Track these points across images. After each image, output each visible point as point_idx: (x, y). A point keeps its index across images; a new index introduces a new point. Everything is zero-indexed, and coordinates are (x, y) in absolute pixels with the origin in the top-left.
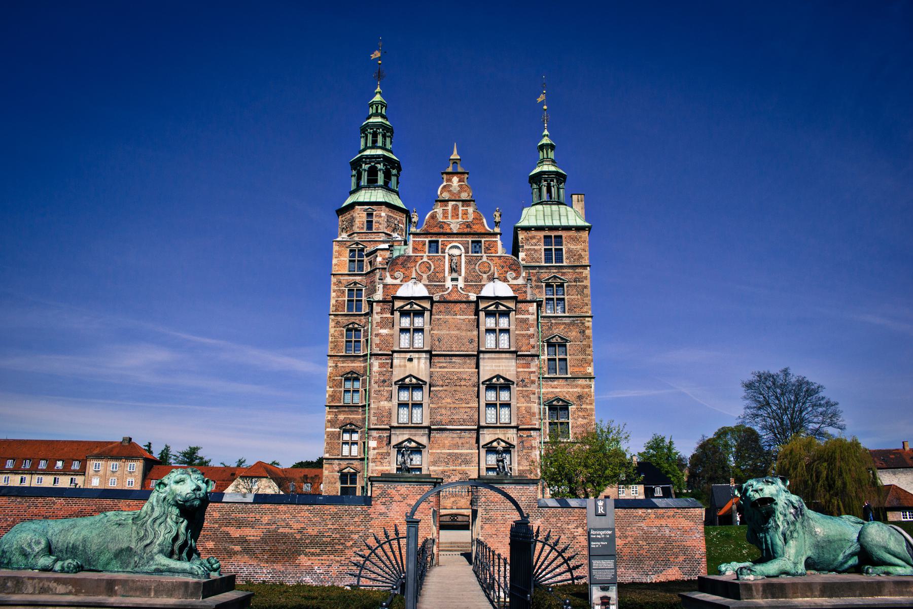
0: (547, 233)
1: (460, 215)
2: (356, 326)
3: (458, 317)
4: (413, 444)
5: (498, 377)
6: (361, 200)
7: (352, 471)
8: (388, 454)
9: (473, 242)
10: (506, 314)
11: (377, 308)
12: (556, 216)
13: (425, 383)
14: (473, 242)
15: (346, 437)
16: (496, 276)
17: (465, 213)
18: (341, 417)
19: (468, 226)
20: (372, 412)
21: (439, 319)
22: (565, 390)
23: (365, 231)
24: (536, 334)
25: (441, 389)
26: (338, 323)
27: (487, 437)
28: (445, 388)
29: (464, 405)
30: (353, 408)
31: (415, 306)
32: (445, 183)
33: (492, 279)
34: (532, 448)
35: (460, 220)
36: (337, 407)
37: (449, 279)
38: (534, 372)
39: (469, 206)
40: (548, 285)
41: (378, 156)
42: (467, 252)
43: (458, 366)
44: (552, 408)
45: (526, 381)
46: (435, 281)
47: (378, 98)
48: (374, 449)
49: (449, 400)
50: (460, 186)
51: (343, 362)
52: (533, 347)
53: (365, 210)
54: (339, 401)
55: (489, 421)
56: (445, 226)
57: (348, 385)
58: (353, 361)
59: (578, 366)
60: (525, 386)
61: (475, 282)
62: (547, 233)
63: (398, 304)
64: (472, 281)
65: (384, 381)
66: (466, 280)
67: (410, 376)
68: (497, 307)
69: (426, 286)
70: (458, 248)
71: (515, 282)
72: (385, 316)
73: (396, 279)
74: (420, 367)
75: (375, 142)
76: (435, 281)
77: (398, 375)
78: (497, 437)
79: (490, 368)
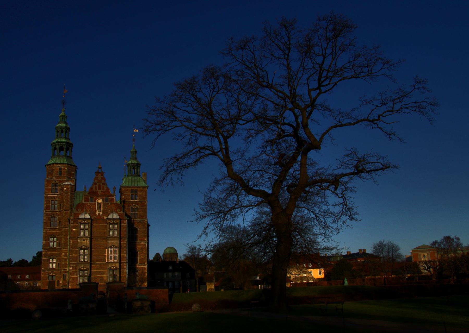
6: (57, 162)
11: (72, 221)
17: (103, 188)
30: (54, 249)
33: (112, 212)
36: (47, 249)
40: (132, 208)
41: (64, 142)
42: (103, 202)
46: (92, 213)
57: (52, 239)
61: (106, 213)
62: (132, 189)
63: (80, 221)
66: (103, 212)
69: (89, 214)
71: (120, 213)
76: (92, 213)
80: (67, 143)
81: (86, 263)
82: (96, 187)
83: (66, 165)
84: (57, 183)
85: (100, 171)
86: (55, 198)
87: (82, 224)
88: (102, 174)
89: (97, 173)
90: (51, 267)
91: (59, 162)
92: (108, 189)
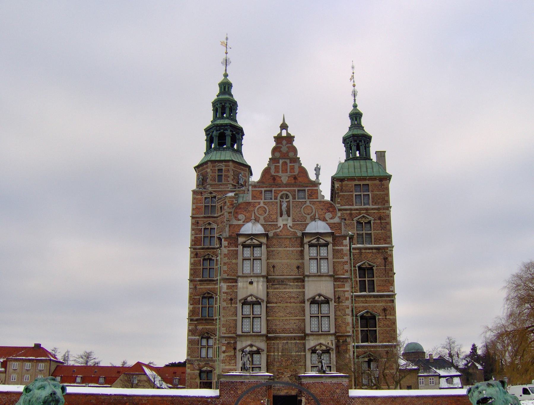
0: (357, 182)
1: (289, 170)
2: (210, 257)
3: (288, 249)
4: (255, 349)
5: (320, 295)
7: (209, 369)
8: (235, 356)
9: (298, 190)
10: (326, 245)
11: (225, 243)
12: (364, 169)
13: (263, 301)
14: (298, 190)
15: (204, 342)
16: (317, 216)
17: (292, 168)
18: (200, 327)
19: (295, 178)
20: (222, 323)
21: (272, 251)
22: (374, 304)
23: (217, 183)
24: (349, 261)
25: (275, 305)
26: (197, 254)
27: (311, 343)
28: (279, 305)
29: (293, 318)
31: (254, 241)
33: (313, 219)
35: (288, 173)
36: (197, 320)
37: (280, 219)
38: (348, 291)
40: (358, 222)
41: (226, 125)
43: (288, 286)
45: (342, 298)
48: (224, 352)
49: (281, 314)
50: (288, 147)
51: (201, 285)
52: (347, 272)
54: (198, 315)
55: (313, 329)
56: (277, 178)
58: (208, 284)
59: (383, 286)
60: (341, 302)
62: (357, 182)
63: (241, 240)
64: (298, 221)
65: (231, 300)
67: (251, 295)
68: (318, 241)
69: (262, 225)
71: (332, 221)
72: (231, 249)
73: (239, 220)
74: (259, 289)
77: (241, 295)
78: (319, 342)
79: (312, 289)
80: (231, 126)
81: (258, 335)
82: (277, 168)
83: (231, 163)
84: (215, 197)
85: (284, 133)
86: (209, 224)
87: (249, 246)
88: (290, 138)
89: (278, 139)
90: (204, 354)
91: (218, 159)
92: (304, 172)
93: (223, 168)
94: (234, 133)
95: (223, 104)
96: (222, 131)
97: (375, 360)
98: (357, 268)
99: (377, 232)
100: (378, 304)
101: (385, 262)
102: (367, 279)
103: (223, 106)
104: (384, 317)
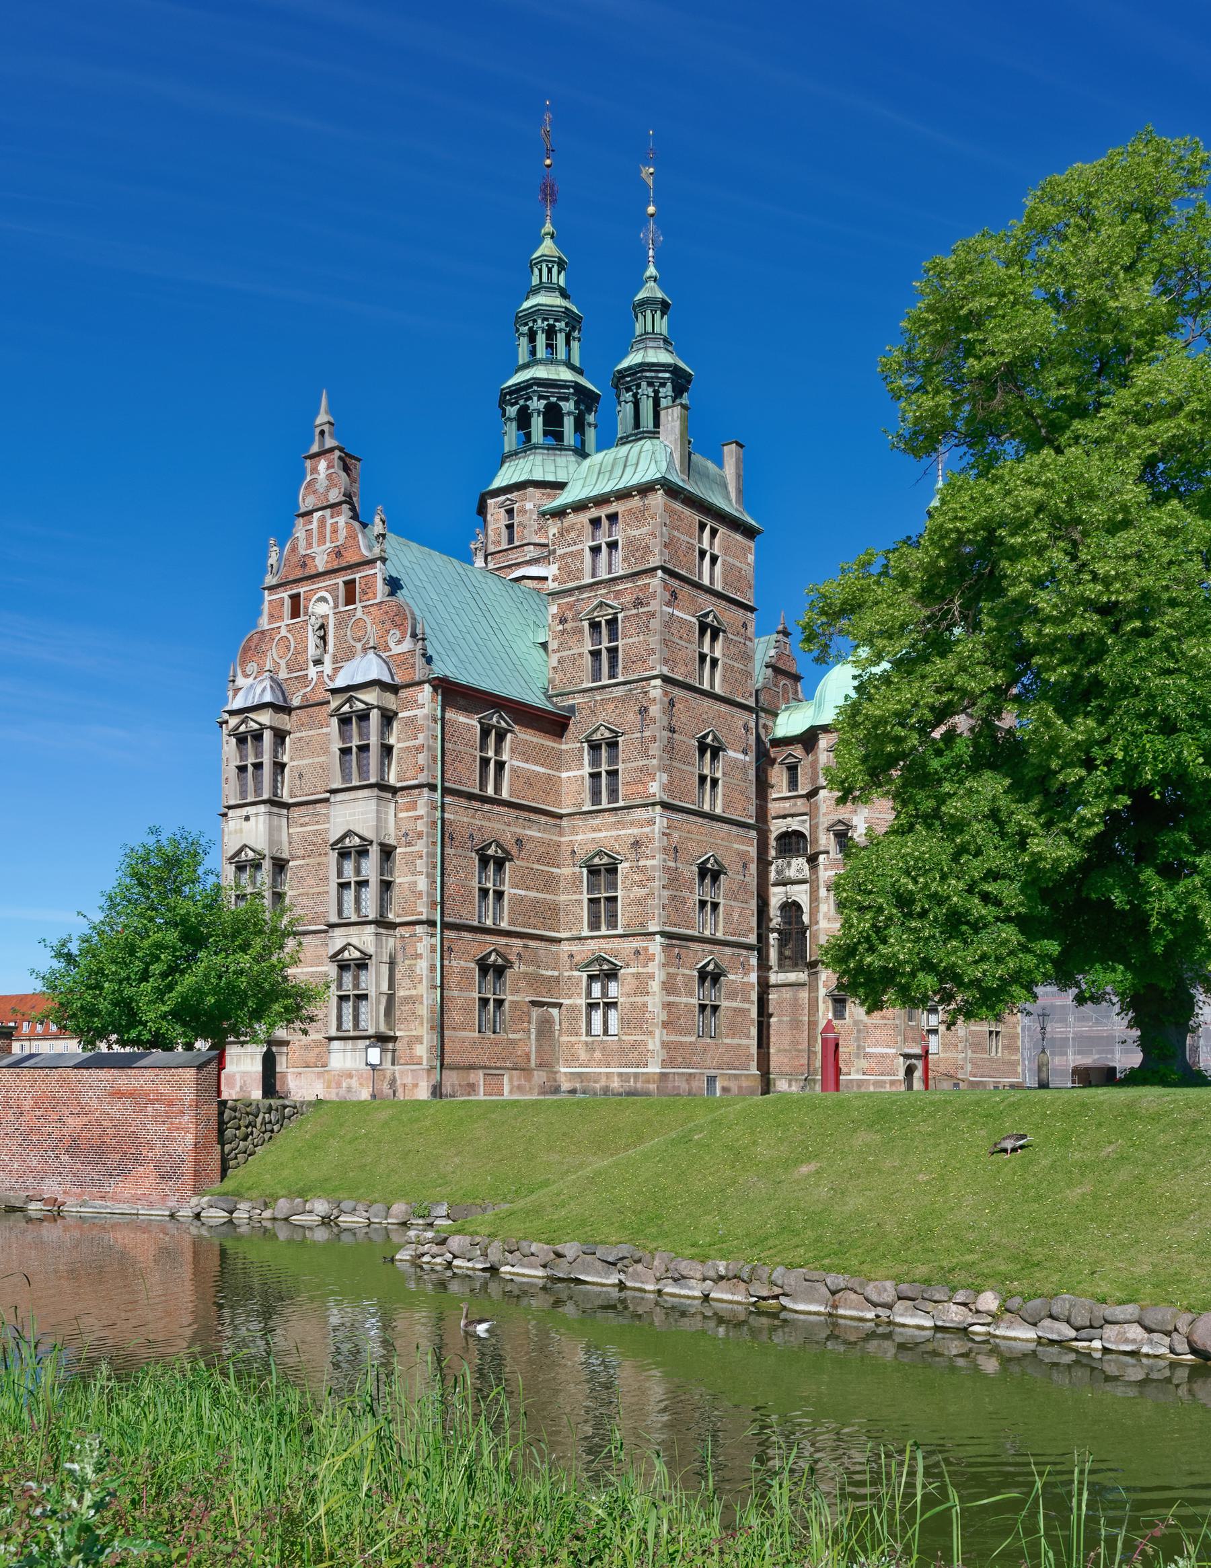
5: (349, 834)
17: (335, 531)
22: (614, 833)
32: (308, 478)
33: (365, 650)
34: (419, 956)
39: (339, 514)
40: (595, 626)
42: (336, 606)
44: (593, 871)
47: (547, 248)
50: (329, 477)
53: (501, 506)
60: (409, 844)
70: (323, 599)
75: (533, 352)
93: (515, 506)
94: (553, 399)
95: (531, 324)
96: (522, 402)
97: (611, 975)
98: (585, 745)
99: (630, 640)
100: (622, 832)
101: (643, 719)
102: (604, 767)
103: (531, 329)
104: (634, 864)
